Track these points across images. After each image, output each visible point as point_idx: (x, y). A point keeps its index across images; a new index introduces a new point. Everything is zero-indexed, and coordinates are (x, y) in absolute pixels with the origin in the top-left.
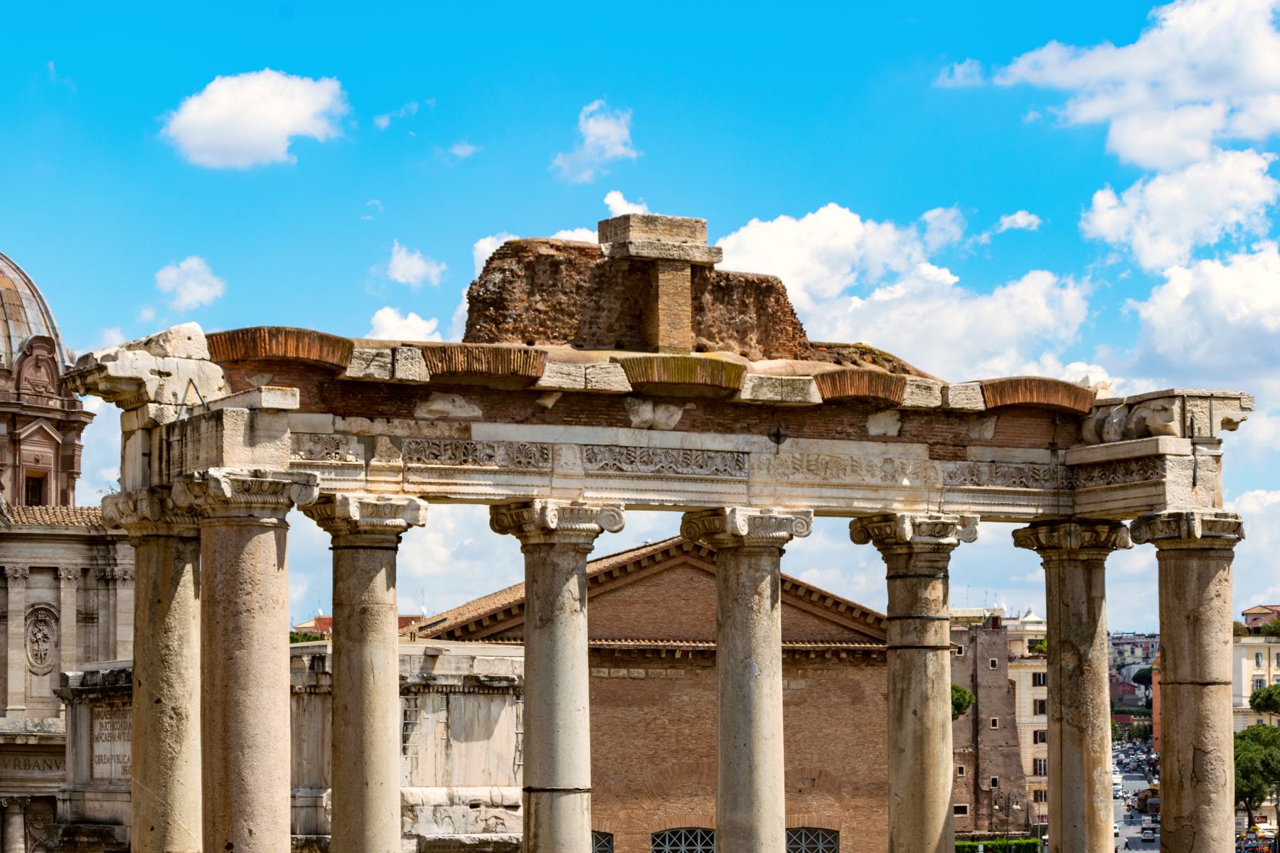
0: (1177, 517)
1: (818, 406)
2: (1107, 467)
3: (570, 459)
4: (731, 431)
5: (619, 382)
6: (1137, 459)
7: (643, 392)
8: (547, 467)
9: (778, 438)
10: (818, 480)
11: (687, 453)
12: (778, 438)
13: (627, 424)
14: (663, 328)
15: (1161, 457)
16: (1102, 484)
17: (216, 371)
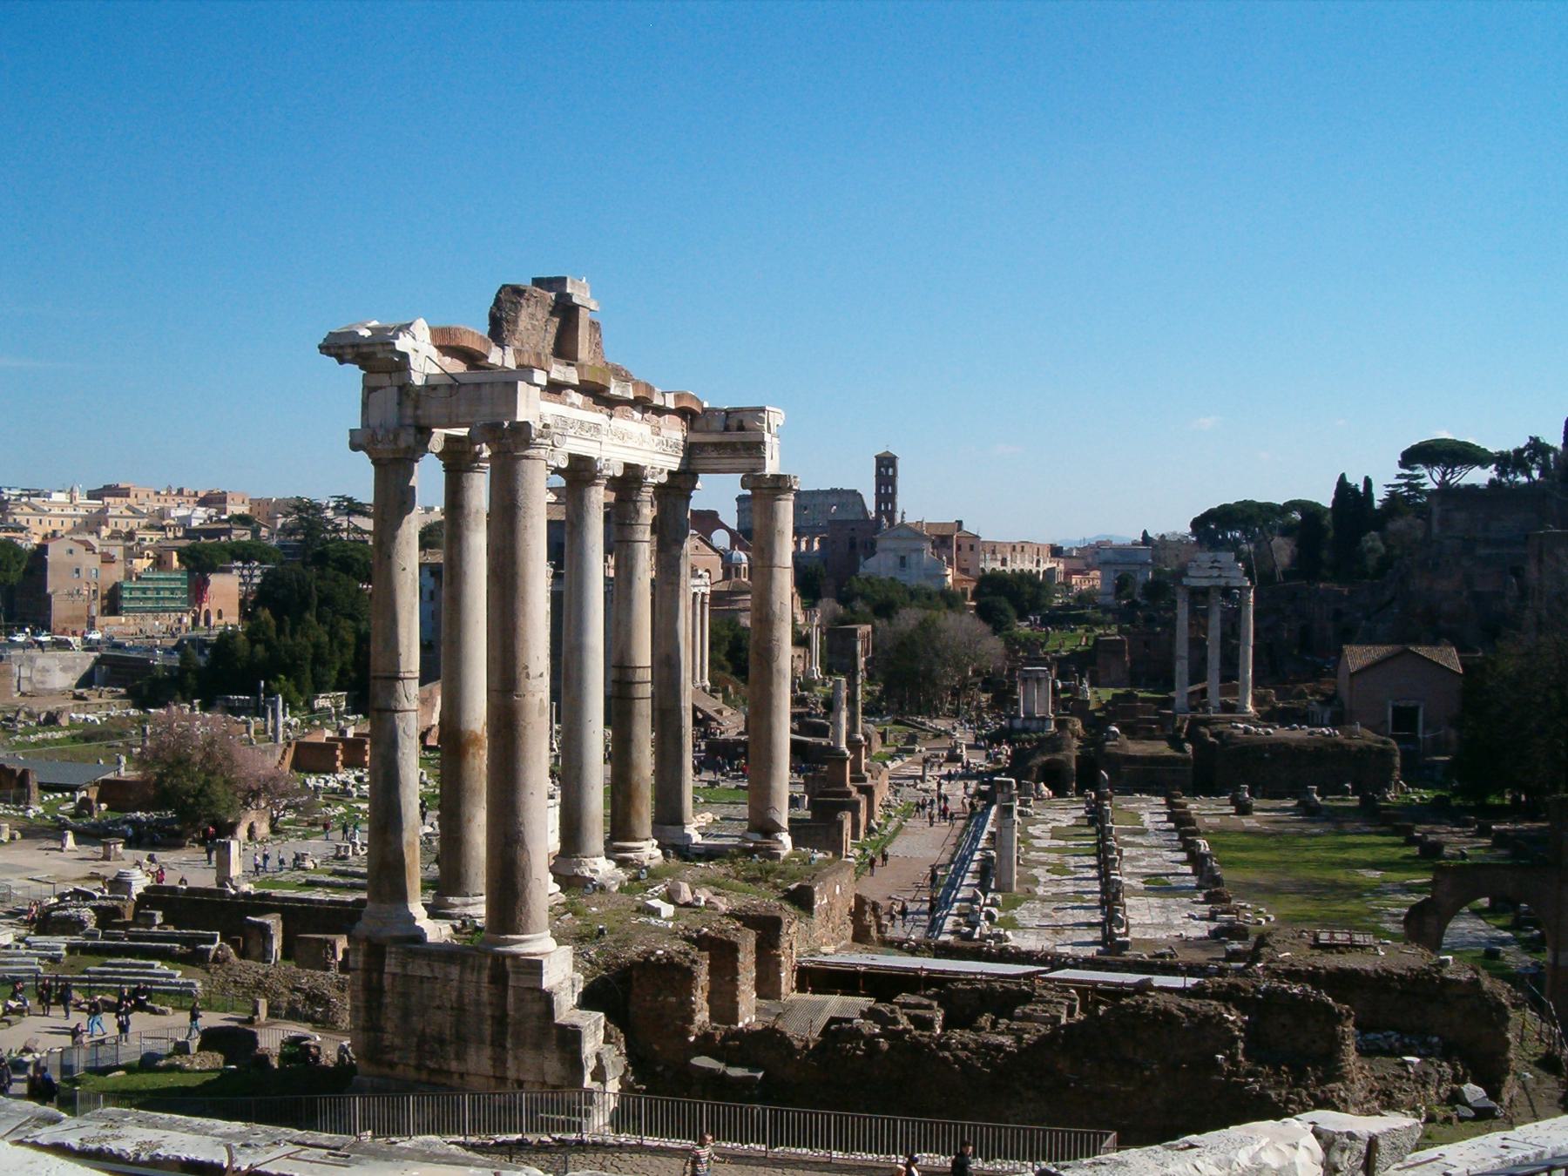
0: (777, 478)
2: (717, 446)
5: (573, 376)
11: (582, 423)
13: (563, 403)
15: (763, 443)
16: (714, 454)
17: (434, 353)
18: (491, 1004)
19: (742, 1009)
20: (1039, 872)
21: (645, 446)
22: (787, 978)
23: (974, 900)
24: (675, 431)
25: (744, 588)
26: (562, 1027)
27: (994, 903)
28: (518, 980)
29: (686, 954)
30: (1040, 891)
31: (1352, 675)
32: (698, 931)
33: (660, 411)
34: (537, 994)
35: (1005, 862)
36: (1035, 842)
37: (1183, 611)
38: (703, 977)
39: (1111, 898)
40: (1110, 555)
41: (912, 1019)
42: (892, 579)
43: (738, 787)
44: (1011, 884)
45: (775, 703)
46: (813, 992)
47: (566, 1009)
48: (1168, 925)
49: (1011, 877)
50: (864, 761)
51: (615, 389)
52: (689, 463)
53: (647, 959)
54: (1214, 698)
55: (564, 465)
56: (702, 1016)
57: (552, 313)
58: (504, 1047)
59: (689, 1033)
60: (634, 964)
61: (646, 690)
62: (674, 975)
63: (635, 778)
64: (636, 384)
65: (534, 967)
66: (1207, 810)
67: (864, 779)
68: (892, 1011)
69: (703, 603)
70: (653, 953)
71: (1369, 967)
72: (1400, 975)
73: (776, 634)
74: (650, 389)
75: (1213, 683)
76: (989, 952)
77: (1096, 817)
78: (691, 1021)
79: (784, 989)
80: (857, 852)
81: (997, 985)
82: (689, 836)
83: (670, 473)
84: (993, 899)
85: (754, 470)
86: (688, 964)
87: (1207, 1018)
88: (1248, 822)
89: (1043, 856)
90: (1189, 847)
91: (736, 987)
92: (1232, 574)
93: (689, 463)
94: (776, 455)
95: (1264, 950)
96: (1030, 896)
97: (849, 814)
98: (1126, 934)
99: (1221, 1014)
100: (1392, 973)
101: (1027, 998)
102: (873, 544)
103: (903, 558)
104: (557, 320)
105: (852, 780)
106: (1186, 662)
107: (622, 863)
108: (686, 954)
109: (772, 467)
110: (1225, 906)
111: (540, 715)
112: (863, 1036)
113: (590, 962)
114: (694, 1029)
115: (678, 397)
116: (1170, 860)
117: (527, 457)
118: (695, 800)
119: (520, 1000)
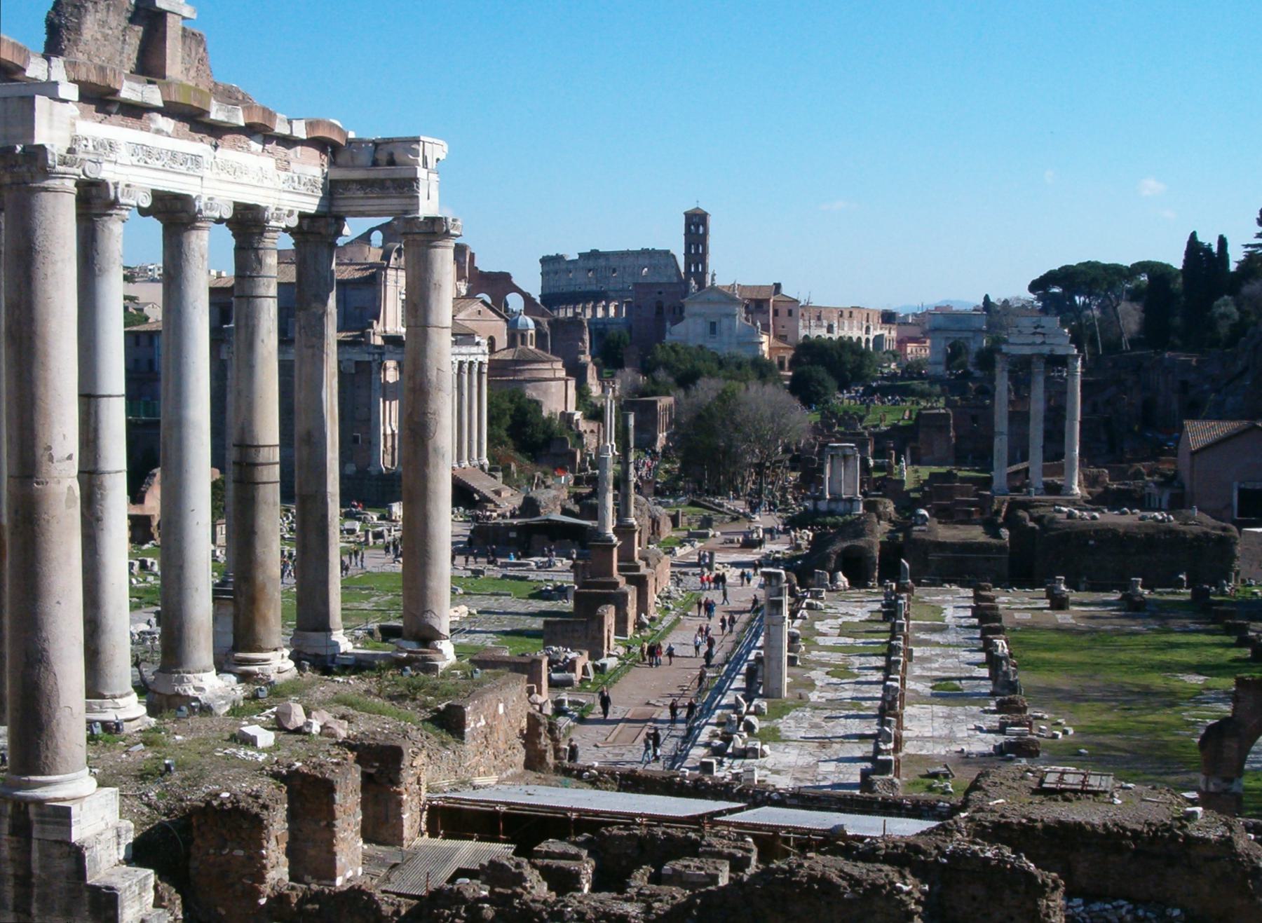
0: (433, 221)
1: (241, 127)
2: (364, 184)
3: (123, 155)
4: (194, 140)
5: (154, 96)
6: (394, 180)
7: (169, 110)
8: (113, 157)
9: (216, 147)
10: (231, 178)
11: (174, 155)
12: (216, 147)
14: (168, 61)
15: (416, 180)
16: (360, 194)
18: (12, 860)
19: (341, 860)
20: (818, 675)
21: (267, 183)
22: (412, 820)
23: (735, 707)
24: (312, 166)
25: (532, 356)
26: (95, 889)
27: (758, 712)
28: (43, 830)
29: (257, 797)
30: (814, 696)
31: (1193, 454)
32: (289, 766)
33: (288, 142)
34: (67, 849)
35: (774, 664)
36: (821, 641)
37: (1002, 384)
38: (278, 824)
39: (889, 709)
40: (940, 321)
41: (546, 873)
42: (701, 347)
43: (505, 576)
44: (780, 690)
45: (431, 486)
46: (444, 838)
47: (106, 861)
48: (951, 739)
49: (781, 680)
50: (637, 548)
51: (217, 113)
52: (331, 205)
53: (208, 803)
54: (1038, 479)
55: (146, 203)
56: (278, 872)
57: (132, 20)
58: (29, 914)
59: (259, 894)
60: (195, 811)
61: (275, 473)
62: (241, 823)
63: (260, 578)
64: (249, 108)
65: (62, 816)
66: (1017, 604)
67: (637, 568)
68: (518, 865)
69: (480, 373)
70: (217, 795)
71: (1097, 820)
72: (1134, 831)
73: (432, 406)
74: (271, 115)
75: (1036, 462)
76: (682, 784)
77: (891, 611)
78: (261, 879)
79: (407, 833)
80: (621, 650)
81: (659, 831)
82: (336, 644)
83: (303, 216)
84: (757, 707)
85: (406, 212)
86: (256, 810)
87: (876, 888)
88: (1063, 618)
89: (826, 656)
90: (988, 647)
91: (333, 835)
92: (1058, 340)
93: (331, 205)
94: (435, 194)
95: (976, 795)
96: (802, 702)
97: (612, 609)
98: (896, 750)
99: (892, 883)
100: (1125, 829)
101: (692, 848)
102: (682, 310)
103: (713, 325)
104: (139, 29)
105: (620, 569)
106: (1005, 438)
107: (244, 678)
108: (257, 797)
109: (428, 207)
110: (1015, 717)
111: (69, 507)
112: (464, 900)
113: (149, 805)
114: (266, 889)
115: (311, 125)
116: (963, 661)
117: (46, 190)
118: (453, 591)
119: (45, 855)
